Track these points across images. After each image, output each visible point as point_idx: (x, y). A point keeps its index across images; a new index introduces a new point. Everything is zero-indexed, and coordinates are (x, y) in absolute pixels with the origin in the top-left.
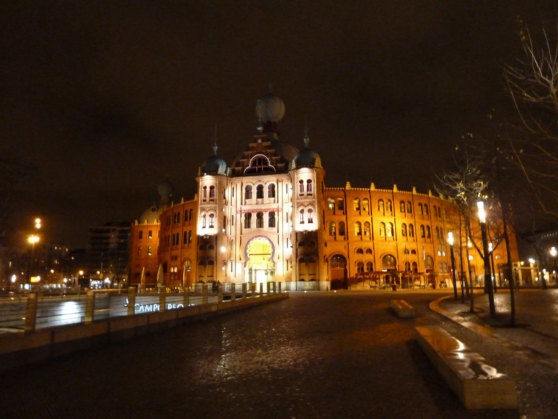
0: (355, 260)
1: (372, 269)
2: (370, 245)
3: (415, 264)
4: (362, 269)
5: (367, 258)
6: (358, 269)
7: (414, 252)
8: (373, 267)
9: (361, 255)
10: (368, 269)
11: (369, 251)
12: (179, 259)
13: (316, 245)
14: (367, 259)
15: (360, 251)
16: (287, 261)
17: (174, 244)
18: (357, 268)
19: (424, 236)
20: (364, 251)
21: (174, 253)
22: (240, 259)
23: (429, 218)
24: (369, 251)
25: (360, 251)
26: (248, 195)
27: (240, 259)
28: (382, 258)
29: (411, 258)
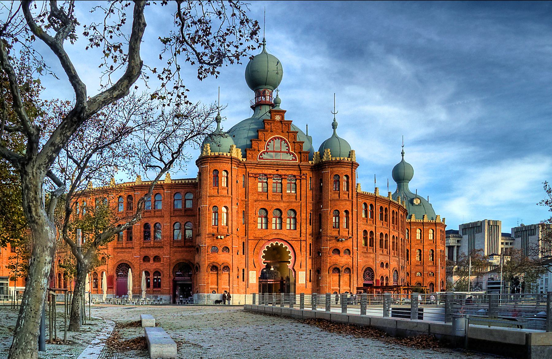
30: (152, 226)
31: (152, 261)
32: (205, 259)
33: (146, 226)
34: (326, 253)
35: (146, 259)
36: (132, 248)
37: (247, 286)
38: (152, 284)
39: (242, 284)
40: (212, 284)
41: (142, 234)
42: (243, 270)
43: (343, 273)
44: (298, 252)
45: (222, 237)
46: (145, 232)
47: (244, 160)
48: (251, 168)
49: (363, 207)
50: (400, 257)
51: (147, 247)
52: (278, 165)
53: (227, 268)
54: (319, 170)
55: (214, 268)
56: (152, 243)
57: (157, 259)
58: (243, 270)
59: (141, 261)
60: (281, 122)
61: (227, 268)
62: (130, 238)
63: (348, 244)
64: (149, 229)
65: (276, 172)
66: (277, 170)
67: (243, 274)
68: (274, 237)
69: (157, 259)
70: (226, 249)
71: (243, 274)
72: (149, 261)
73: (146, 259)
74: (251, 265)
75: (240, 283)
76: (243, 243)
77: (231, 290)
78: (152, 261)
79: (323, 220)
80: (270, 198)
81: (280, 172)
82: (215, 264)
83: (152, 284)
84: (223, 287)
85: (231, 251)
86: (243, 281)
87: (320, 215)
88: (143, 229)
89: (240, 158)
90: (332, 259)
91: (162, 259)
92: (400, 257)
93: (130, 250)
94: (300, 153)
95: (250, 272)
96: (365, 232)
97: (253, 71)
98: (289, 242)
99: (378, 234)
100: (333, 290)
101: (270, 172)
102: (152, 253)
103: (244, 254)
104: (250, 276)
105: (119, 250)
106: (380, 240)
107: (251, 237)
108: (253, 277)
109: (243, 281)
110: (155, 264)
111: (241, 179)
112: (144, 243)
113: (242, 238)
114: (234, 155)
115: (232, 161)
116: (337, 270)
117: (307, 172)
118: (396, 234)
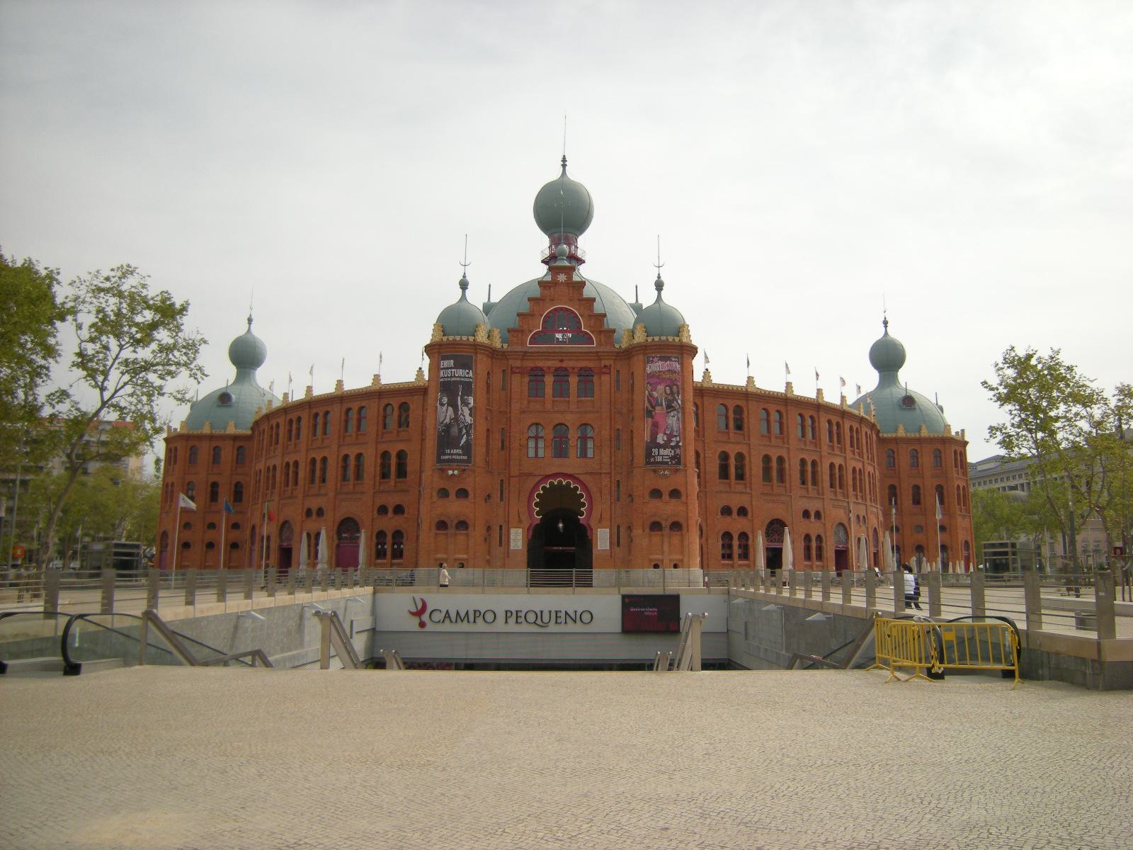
2: (743, 501)
4: (730, 546)
6: (723, 545)
8: (750, 542)
9: (728, 519)
10: (740, 546)
11: (743, 511)
12: (329, 515)
13: (683, 498)
15: (726, 511)
16: (618, 527)
17: (312, 481)
18: (721, 542)
19: (832, 486)
21: (314, 504)
22: (520, 521)
23: (843, 450)
24: (743, 511)
25: (726, 511)
26: (536, 390)
27: (520, 521)
29: (814, 528)
31: (390, 514)
33: (385, 455)
36: (363, 493)
37: (508, 553)
38: (389, 553)
41: (378, 469)
42: (501, 526)
45: (456, 472)
47: (505, 346)
48: (516, 359)
49: (764, 414)
50: (868, 503)
51: (382, 492)
53: (463, 525)
54: (629, 358)
55: (442, 525)
56: (392, 483)
57: (399, 510)
58: (501, 526)
61: (463, 525)
62: (359, 475)
63: (676, 481)
64: (390, 459)
65: (558, 364)
66: (561, 361)
68: (554, 470)
69: (399, 510)
70: (463, 493)
73: (383, 510)
76: (502, 480)
78: (390, 514)
80: (549, 406)
81: (564, 365)
82: (443, 519)
83: (389, 553)
86: (501, 544)
87: (632, 431)
88: (379, 461)
89: (497, 343)
92: (868, 503)
95: (513, 531)
96: (767, 459)
98: (581, 477)
101: (550, 363)
102: (391, 501)
103: (502, 500)
107: (515, 471)
108: (517, 539)
109: (501, 544)
110: (397, 517)
111: (497, 379)
112: (380, 483)
114: (481, 337)
115: (476, 349)
117: (611, 362)
118: (838, 461)
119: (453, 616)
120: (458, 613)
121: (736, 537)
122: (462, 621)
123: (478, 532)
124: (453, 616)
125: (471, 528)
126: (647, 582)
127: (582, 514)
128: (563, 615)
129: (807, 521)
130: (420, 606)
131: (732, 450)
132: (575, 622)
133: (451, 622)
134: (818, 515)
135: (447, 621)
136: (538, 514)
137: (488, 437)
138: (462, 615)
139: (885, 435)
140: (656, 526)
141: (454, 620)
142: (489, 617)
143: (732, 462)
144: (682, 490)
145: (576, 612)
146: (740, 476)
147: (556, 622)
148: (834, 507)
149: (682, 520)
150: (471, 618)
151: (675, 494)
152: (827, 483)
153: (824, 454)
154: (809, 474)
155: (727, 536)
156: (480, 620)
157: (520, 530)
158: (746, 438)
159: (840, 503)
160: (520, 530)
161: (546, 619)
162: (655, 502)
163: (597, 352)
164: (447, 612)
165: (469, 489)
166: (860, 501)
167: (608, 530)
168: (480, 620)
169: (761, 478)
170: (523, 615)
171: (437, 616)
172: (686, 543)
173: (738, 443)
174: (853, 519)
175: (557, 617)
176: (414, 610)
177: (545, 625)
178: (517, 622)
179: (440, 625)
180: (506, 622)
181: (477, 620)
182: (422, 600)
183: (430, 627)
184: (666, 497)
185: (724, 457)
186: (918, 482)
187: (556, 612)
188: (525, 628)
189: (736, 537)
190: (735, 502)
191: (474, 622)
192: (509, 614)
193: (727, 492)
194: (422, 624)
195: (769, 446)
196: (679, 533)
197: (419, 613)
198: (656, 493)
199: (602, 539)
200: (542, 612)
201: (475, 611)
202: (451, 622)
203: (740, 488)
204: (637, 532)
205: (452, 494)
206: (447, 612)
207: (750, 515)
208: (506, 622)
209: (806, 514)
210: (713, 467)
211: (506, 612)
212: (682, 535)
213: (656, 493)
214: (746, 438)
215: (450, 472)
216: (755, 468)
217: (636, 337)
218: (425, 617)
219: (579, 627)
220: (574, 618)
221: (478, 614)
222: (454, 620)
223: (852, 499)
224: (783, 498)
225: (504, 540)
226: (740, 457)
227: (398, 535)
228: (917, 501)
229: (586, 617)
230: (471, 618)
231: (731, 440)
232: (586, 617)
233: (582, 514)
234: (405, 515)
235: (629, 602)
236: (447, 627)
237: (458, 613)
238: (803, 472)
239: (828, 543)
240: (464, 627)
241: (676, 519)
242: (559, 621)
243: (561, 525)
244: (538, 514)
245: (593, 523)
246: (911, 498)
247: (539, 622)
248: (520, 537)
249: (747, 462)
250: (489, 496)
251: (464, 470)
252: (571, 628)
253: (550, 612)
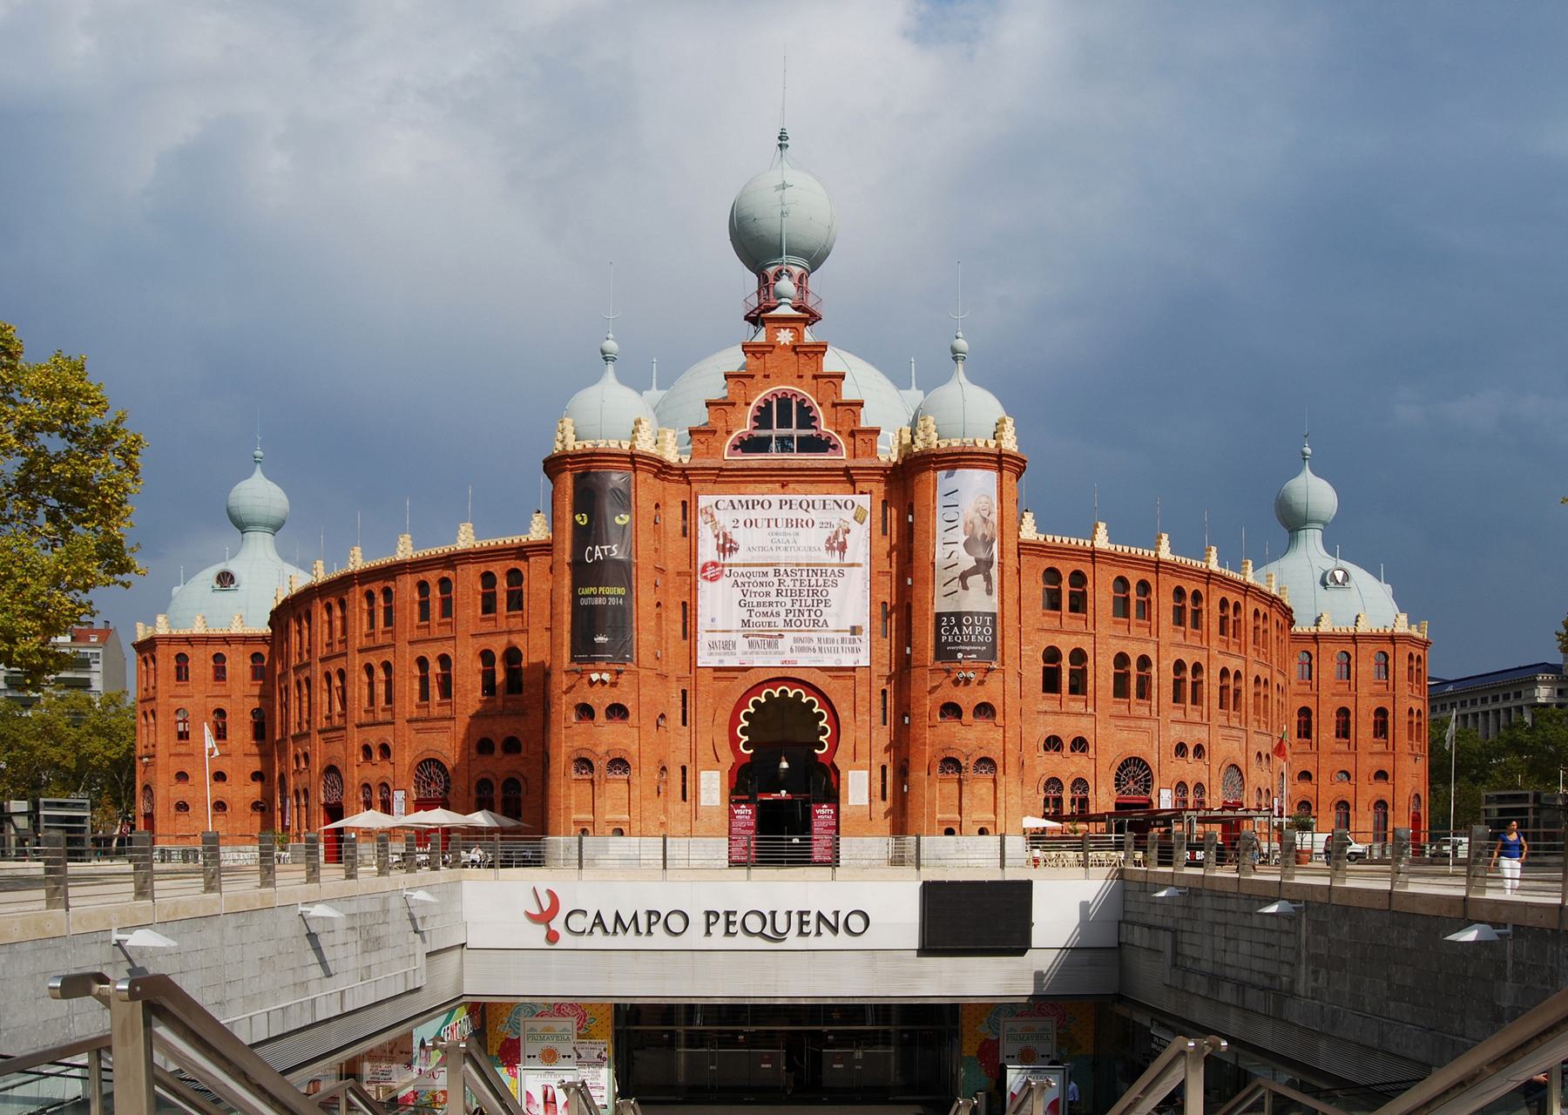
0: (1040, 770)
1: (1084, 802)
2: (1083, 727)
3: (1199, 787)
4: (1058, 802)
5: (1069, 766)
7: (1199, 751)
9: (1056, 757)
11: (1080, 744)
13: (999, 718)
14: (1073, 769)
15: (1053, 743)
20: (1067, 743)
24: (1080, 744)
25: (1053, 743)
28: (1114, 771)
30: (498, 654)
31: (498, 752)
32: (568, 737)
34: (922, 715)
35: (485, 746)
37: (695, 814)
39: (677, 807)
40: (579, 810)
42: (684, 769)
43: (970, 773)
44: (844, 715)
46: (484, 673)
52: (783, 469)
53: (619, 764)
58: (684, 769)
59: (473, 751)
60: (794, 348)
61: (619, 764)
67: (684, 780)
70: (618, 711)
71: (684, 780)
72: (492, 751)
74: (705, 752)
75: (670, 806)
76: (684, 692)
77: (636, 827)
78: (498, 752)
79: (915, 622)
82: (585, 755)
84: (608, 817)
85: (633, 717)
86: (684, 798)
90: (936, 735)
91: (524, 746)
93: (446, 723)
94: (852, 434)
95: (704, 775)
97: (740, 220)
99: (1168, 665)
100: (941, 822)
103: (684, 723)
104: (703, 785)
105: (420, 725)
106: (1222, 688)
108: (712, 787)
109: (684, 798)
110: (508, 758)
113: (679, 679)
116: (951, 764)
119: (609, 922)
120: (618, 917)
121: (1067, 786)
122: (626, 930)
123: (644, 776)
124: (609, 922)
125: (634, 771)
126: (969, 859)
127: (822, 746)
128: (812, 918)
129: (1181, 762)
130: (546, 905)
131: (1066, 645)
132: (835, 930)
133: (606, 931)
134: (1199, 751)
135: (598, 930)
136: (746, 746)
137: (659, 615)
138: (627, 919)
139: (1299, 630)
140: (951, 764)
141: (610, 928)
142: (676, 923)
143: (1066, 665)
144: (998, 704)
145: (837, 913)
146: (1078, 686)
147: (801, 933)
148: (1226, 738)
149: (996, 755)
150: (643, 927)
151: (985, 710)
152: (1215, 702)
153: (1214, 652)
154: (1187, 684)
155: (1054, 783)
156: (658, 929)
157: (717, 774)
158: (1090, 625)
159: (1234, 732)
160: (717, 774)
161: (781, 928)
162: (952, 726)
163: (847, 469)
164: (598, 915)
165: (628, 705)
166: (1263, 729)
167: (866, 773)
168: (658, 929)
169: (1111, 693)
170: (738, 918)
171: (578, 923)
172: (1000, 795)
173: (1075, 633)
174: (1253, 756)
175: (802, 923)
176: (536, 911)
177: (779, 937)
178: (728, 933)
179: (585, 937)
180: (708, 933)
181: (653, 929)
182: (551, 894)
183: (566, 941)
184: (967, 716)
185: (1052, 655)
186: (1348, 703)
187: (801, 913)
188: (741, 941)
189: (1067, 786)
190: (1068, 729)
191: (649, 932)
192: (712, 919)
193: (1056, 713)
194: (552, 937)
195: (1125, 638)
196: (991, 776)
197: (544, 917)
198: (951, 710)
199: (857, 787)
200: (773, 913)
201: (650, 913)
202: (606, 931)
203: (1078, 706)
204: (918, 775)
205: (600, 714)
206: (598, 915)
207: (1092, 750)
208: (708, 933)
209: (1181, 749)
210: (1035, 671)
211: (708, 913)
212: (995, 781)
213: (951, 710)
214: (1090, 625)
215: (595, 677)
216: (1102, 674)
217: (918, 442)
218: (557, 924)
219: (842, 939)
220: (832, 920)
221: (654, 919)
222: (609, 925)
223: (1253, 726)
224: (1144, 724)
225: (687, 792)
226: (1078, 656)
227: (511, 784)
228: (1343, 731)
229: (856, 923)
230: (643, 927)
231: (1065, 628)
232: (856, 923)
233: (822, 746)
234: (523, 754)
235: (936, 897)
236: (598, 940)
237: (618, 917)
238: (1178, 685)
239: (1214, 797)
240: (628, 940)
241: (983, 754)
242: (806, 929)
243: (785, 765)
244: (746, 746)
245: (839, 760)
246: (1333, 727)
247: (768, 931)
248: (717, 785)
249: (1090, 665)
250: (662, 716)
251: (619, 673)
252: (827, 939)
253: (789, 913)
